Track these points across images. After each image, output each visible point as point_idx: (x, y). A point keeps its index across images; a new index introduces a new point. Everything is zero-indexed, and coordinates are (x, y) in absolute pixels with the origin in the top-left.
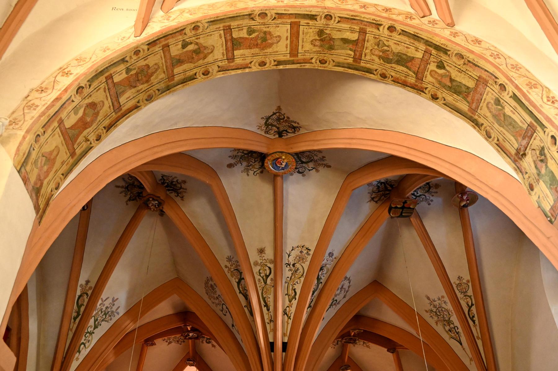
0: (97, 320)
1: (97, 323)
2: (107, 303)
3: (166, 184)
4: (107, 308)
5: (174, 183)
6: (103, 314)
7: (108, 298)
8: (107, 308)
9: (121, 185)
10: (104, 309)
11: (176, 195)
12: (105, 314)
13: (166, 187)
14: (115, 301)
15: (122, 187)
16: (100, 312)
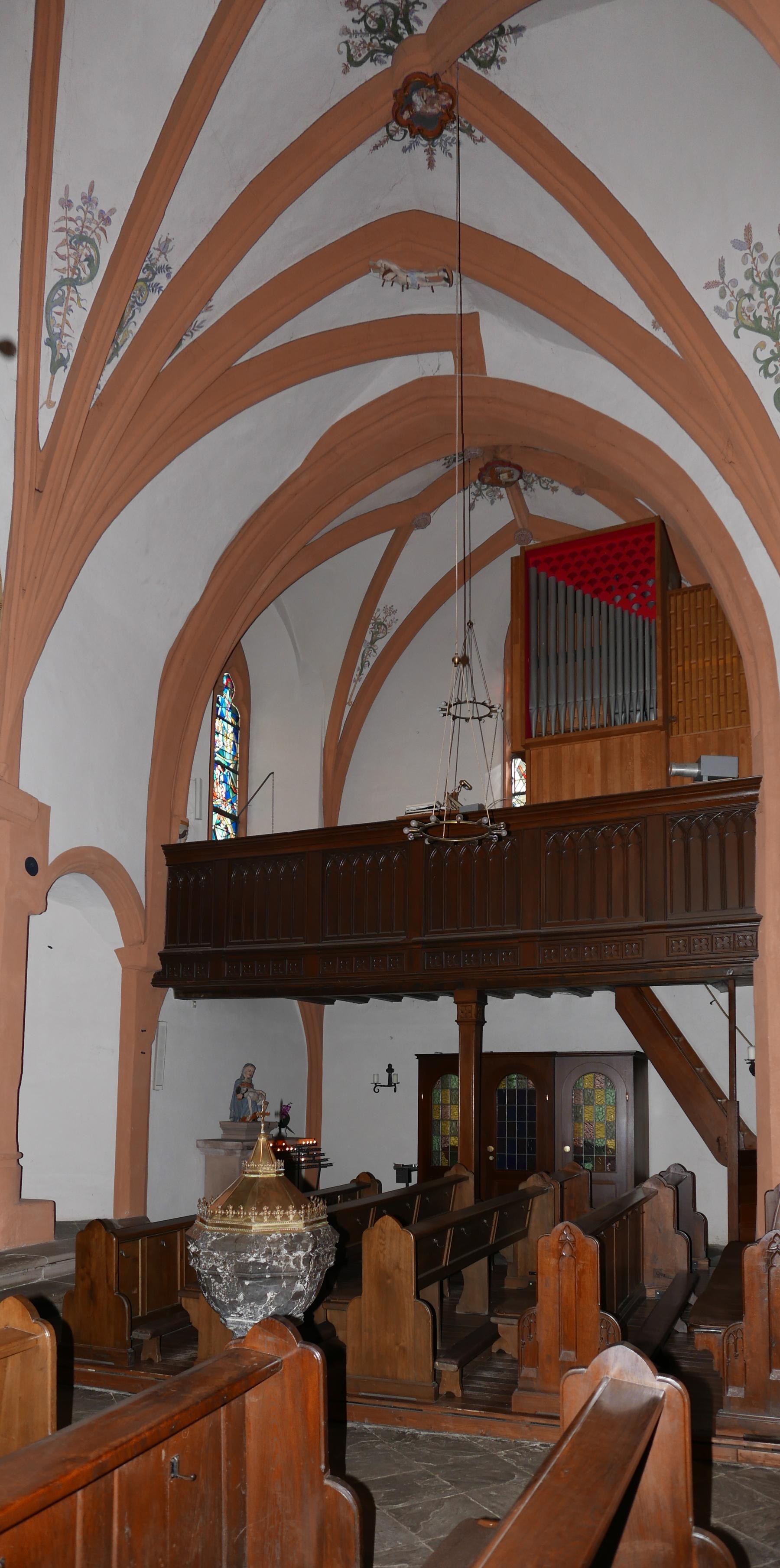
0: (758, 320)
1: (765, 324)
2: (736, 270)
3: (389, 43)
4: (749, 275)
5: (373, 25)
6: (757, 294)
7: (722, 262)
8: (749, 275)
9: (425, 156)
10: (746, 285)
11: (417, 7)
12: (763, 286)
13: (398, 38)
14: (749, 239)
15: (430, 152)
16: (745, 303)
